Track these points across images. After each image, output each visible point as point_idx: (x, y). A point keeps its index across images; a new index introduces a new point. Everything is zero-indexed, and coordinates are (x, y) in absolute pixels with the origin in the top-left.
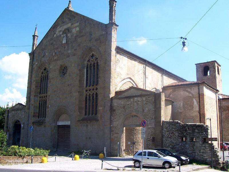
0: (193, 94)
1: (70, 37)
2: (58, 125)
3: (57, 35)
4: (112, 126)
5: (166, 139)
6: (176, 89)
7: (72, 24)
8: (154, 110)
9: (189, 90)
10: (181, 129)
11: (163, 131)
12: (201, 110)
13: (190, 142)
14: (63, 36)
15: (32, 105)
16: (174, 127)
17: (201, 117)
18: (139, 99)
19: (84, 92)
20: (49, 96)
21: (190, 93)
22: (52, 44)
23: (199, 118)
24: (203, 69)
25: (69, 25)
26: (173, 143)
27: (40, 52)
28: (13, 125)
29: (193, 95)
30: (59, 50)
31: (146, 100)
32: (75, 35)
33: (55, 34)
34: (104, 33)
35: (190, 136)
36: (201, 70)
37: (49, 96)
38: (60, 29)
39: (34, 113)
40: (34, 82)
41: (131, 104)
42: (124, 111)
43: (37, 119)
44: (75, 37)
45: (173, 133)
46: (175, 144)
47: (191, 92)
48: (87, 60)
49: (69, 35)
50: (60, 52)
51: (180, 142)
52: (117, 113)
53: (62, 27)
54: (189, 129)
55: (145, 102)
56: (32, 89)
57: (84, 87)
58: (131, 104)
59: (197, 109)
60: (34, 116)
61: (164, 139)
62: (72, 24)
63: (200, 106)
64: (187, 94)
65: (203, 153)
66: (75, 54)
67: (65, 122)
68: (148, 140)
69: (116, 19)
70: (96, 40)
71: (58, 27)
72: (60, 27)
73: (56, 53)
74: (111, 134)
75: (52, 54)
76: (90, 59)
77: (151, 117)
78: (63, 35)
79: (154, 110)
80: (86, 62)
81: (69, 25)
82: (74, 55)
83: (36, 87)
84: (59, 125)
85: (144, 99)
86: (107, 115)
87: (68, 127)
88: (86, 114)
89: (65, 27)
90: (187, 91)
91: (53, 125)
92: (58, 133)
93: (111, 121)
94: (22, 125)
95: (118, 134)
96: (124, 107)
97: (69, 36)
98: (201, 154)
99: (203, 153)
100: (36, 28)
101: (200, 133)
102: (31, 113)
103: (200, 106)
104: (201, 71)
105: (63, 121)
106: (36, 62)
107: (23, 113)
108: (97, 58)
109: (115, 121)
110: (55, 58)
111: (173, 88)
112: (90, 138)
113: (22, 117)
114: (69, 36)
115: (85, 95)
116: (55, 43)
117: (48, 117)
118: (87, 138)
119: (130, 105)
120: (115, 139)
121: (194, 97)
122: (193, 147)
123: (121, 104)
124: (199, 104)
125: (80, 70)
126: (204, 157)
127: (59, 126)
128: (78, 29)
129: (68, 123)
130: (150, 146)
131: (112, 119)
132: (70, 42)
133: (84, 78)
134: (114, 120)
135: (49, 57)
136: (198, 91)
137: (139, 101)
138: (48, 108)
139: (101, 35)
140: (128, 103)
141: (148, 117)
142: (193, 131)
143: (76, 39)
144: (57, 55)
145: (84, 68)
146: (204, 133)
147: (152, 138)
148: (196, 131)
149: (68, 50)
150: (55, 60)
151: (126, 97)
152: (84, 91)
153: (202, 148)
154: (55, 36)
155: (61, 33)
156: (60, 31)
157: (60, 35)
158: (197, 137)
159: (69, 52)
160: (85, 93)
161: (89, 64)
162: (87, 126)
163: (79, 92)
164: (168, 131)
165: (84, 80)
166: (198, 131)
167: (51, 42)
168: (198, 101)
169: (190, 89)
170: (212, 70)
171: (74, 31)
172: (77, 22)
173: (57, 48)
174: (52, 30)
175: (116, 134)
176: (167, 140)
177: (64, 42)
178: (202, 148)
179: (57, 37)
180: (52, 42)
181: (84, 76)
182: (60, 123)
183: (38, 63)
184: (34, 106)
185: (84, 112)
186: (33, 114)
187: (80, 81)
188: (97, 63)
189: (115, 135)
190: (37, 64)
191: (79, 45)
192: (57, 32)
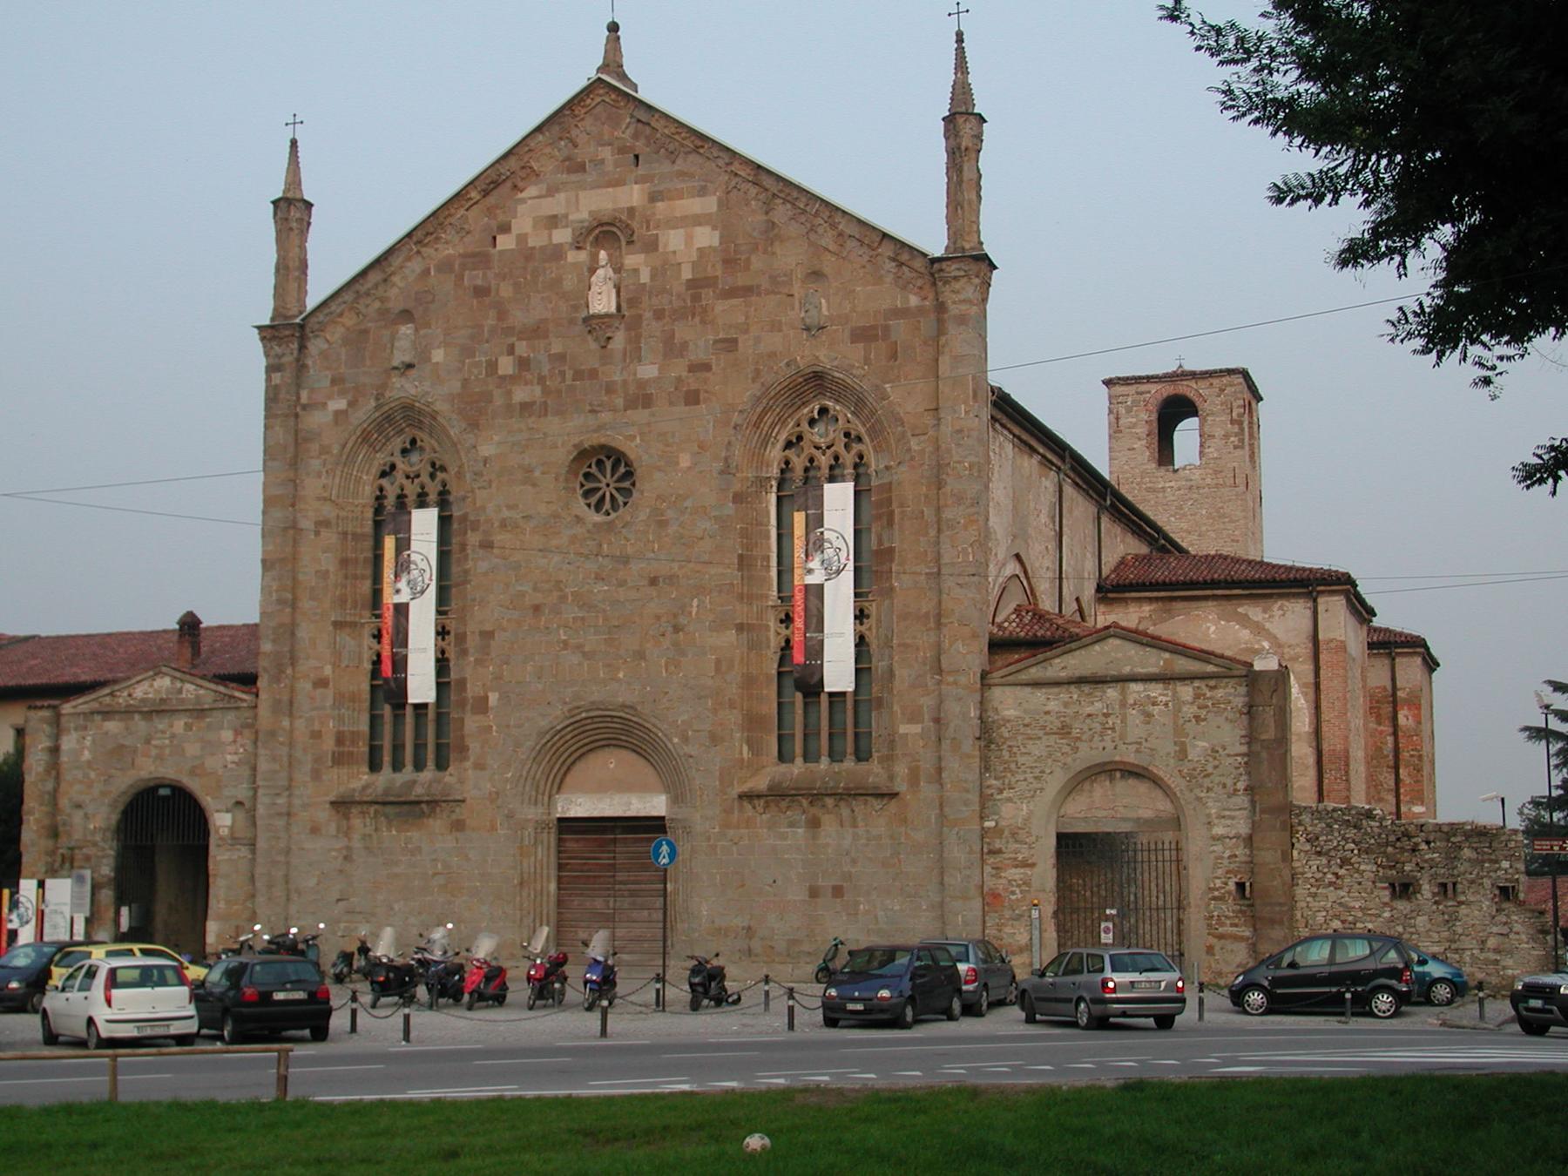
0: (1280, 634)
1: (645, 277)
2: (560, 820)
3: (522, 238)
4: (989, 824)
5: (1313, 890)
6: (1179, 605)
7: (653, 198)
8: (1244, 749)
9: (1254, 612)
10: (1387, 844)
11: (1295, 853)
12: (1325, 728)
13: (1436, 903)
14: (573, 256)
15: (322, 683)
16: (1351, 833)
17: (1326, 766)
18: (1155, 690)
19: (767, 628)
20: (488, 635)
21: (1258, 629)
22: (481, 292)
23: (1312, 773)
24: (1155, 416)
25: (633, 195)
26: (1349, 909)
27: (366, 332)
28: (115, 818)
29: (1280, 646)
30: (557, 348)
31: (1197, 696)
32: (687, 274)
33: (505, 228)
34: (914, 301)
35: (1433, 877)
36: (1143, 420)
37: (488, 635)
39: (340, 739)
40: (330, 537)
41: (1106, 715)
42: (1066, 749)
43: (359, 780)
44: (693, 284)
45: (1345, 862)
46: (1360, 914)
47: (1267, 625)
48: (783, 437)
49: (632, 260)
50: (561, 357)
51: (1386, 904)
52: (1021, 760)
53: (561, 196)
54: (1428, 843)
55: (1189, 710)
56: (307, 576)
57: (767, 597)
58: (1106, 715)
60: (339, 760)
61: (1300, 892)
62: (653, 198)
63: (1317, 707)
64: (1245, 634)
65: (1497, 951)
66: (697, 392)
67: (617, 798)
68: (1214, 898)
69: (995, 233)
70: (863, 335)
71: (532, 191)
72: (551, 192)
73: (523, 364)
74: (988, 869)
75: (492, 366)
76: (800, 438)
77: (1224, 786)
78: (582, 256)
79: (1244, 749)
80: (775, 454)
81: (633, 195)
82: (693, 398)
83: (344, 562)
84: (572, 814)
85: (1186, 691)
86: (961, 769)
87: (654, 826)
88: (783, 757)
89: (594, 202)
90: (1244, 621)
91: (533, 813)
92: (560, 867)
93: (986, 803)
94: (222, 821)
95: (1033, 865)
96: (1064, 731)
97: (636, 271)
98: (1492, 956)
99: (1497, 951)
100: (294, 143)
101: (1483, 861)
102: (316, 735)
103: (1317, 707)
104: (1142, 430)
105: (602, 788)
106: (330, 397)
107: (227, 735)
108: (859, 439)
109: (1010, 800)
110: (520, 394)
111: (1157, 599)
112: (838, 891)
113: (211, 763)
114: (636, 271)
115: (775, 643)
116: (506, 290)
117: (479, 766)
118: (814, 893)
119: (1101, 718)
120: (1013, 893)
122: (1451, 921)
123: (1047, 713)
124: (1312, 695)
125: (738, 498)
126: (1504, 968)
127: (568, 826)
128: (706, 237)
129: (655, 805)
130: (1223, 925)
131: (989, 792)
132: (648, 315)
133: (769, 548)
134: (1005, 794)
135: (465, 382)
136: (1306, 624)
137: (1154, 704)
138: (482, 706)
140: (1089, 710)
141: (1207, 783)
142: (1452, 856)
143: (696, 298)
144: (541, 380)
145: (762, 483)
146: (1505, 864)
147: (1232, 886)
148: (1467, 853)
149: (634, 353)
150: (525, 407)
151: (1080, 681)
152: (771, 624)
153: (1495, 929)
154: (505, 242)
155: (562, 236)
156: (553, 221)
157: (557, 253)
158: (1472, 882)
161: (799, 463)
162: (814, 824)
163: (740, 628)
164: (1319, 853)
165: (768, 558)
166: (1474, 855)
167: (475, 277)
168: (1311, 678)
169: (1265, 611)
170: (1219, 432)
171: (673, 240)
172: (702, 192)
173: (537, 332)
174: (474, 195)
175: (1016, 867)
176: (1314, 896)
177: (602, 301)
178: (1495, 929)
179: (527, 254)
180: (479, 282)
181: (768, 537)
182: (580, 806)
183: (351, 404)
184: (339, 699)
186: (329, 744)
187: (744, 562)
189: (1015, 873)
190: (337, 413)
191: (730, 344)
192: (523, 223)
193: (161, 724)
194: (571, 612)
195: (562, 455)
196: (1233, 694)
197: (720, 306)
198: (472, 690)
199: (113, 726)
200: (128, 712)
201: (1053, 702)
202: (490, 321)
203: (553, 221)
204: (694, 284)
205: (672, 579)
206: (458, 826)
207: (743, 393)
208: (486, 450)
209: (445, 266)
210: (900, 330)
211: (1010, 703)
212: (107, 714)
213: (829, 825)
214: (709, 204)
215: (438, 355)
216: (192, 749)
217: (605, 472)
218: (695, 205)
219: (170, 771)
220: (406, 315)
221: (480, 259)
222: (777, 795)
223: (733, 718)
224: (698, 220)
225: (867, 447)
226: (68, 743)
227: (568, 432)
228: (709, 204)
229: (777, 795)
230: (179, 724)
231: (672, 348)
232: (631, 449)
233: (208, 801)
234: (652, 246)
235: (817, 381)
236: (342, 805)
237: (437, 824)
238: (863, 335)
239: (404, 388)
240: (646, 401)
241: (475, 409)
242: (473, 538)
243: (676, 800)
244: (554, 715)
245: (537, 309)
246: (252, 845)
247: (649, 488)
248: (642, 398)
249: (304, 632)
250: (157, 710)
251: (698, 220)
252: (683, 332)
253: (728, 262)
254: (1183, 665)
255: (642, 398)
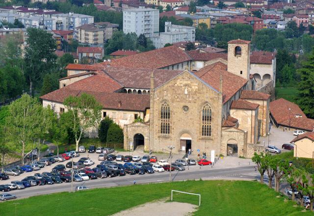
7: (191, 83)
9: (246, 111)
21: (246, 114)
22: (173, 89)
25: (189, 82)
38: (181, 82)
43: (160, 134)
50: (181, 97)
59: (250, 123)
62: (191, 83)
64: (245, 114)
72: (181, 80)
73: (178, 97)
80: (203, 108)
82: (195, 102)
86: (219, 138)
88: (203, 135)
89: (185, 82)
91: (178, 139)
93: (221, 142)
94: (146, 138)
105: (185, 137)
110: (177, 100)
118: (205, 148)
121: (248, 116)
127: (181, 140)
128: (197, 87)
129: (190, 139)
139: (215, 97)
150: (178, 101)
156: (181, 84)
159: (190, 99)
160: (202, 124)
171: (193, 87)
173: (179, 94)
177: (186, 92)
185: (201, 134)
188: (210, 110)
192: (178, 83)
193: (139, 128)
194: (183, 121)
195: (182, 106)
196: (243, 134)
197: (198, 94)
198: (173, 127)
199: (133, 128)
200: (135, 126)
201: (228, 133)
202: (174, 92)
203: (181, 84)
204: (196, 92)
205: (193, 119)
206: (171, 140)
207: (200, 103)
208: (174, 104)
209: (170, 86)
210: (215, 99)
211: (223, 133)
212: (133, 126)
213: (207, 143)
214: (197, 84)
215: (169, 95)
216: (142, 131)
217: (186, 108)
218: (195, 84)
219: (140, 133)
220: (165, 90)
221: (174, 86)
222: (202, 139)
223: (198, 132)
224: (196, 86)
225: (211, 108)
226: (128, 129)
227: (183, 104)
228: (197, 84)
229: (202, 139)
230: (141, 128)
231: (193, 98)
232: (189, 106)
233: (144, 136)
234: (191, 87)
235: (207, 102)
236: (159, 137)
237: (169, 139)
238: (211, 99)
239: (165, 98)
240: (190, 102)
241: (173, 101)
242: (173, 113)
243: (192, 138)
244: (181, 130)
245: (179, 92)
246: (150, 140)
247: (191, 110)
248: (190, 102)
249: (155, 120)
250: (138, 126)
251: (196, 86)
252: (194, 96)
253: (199, 90)
254: (239, 131)
255: (190, 102)
